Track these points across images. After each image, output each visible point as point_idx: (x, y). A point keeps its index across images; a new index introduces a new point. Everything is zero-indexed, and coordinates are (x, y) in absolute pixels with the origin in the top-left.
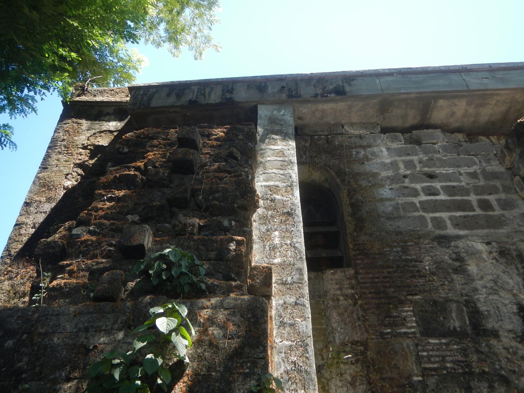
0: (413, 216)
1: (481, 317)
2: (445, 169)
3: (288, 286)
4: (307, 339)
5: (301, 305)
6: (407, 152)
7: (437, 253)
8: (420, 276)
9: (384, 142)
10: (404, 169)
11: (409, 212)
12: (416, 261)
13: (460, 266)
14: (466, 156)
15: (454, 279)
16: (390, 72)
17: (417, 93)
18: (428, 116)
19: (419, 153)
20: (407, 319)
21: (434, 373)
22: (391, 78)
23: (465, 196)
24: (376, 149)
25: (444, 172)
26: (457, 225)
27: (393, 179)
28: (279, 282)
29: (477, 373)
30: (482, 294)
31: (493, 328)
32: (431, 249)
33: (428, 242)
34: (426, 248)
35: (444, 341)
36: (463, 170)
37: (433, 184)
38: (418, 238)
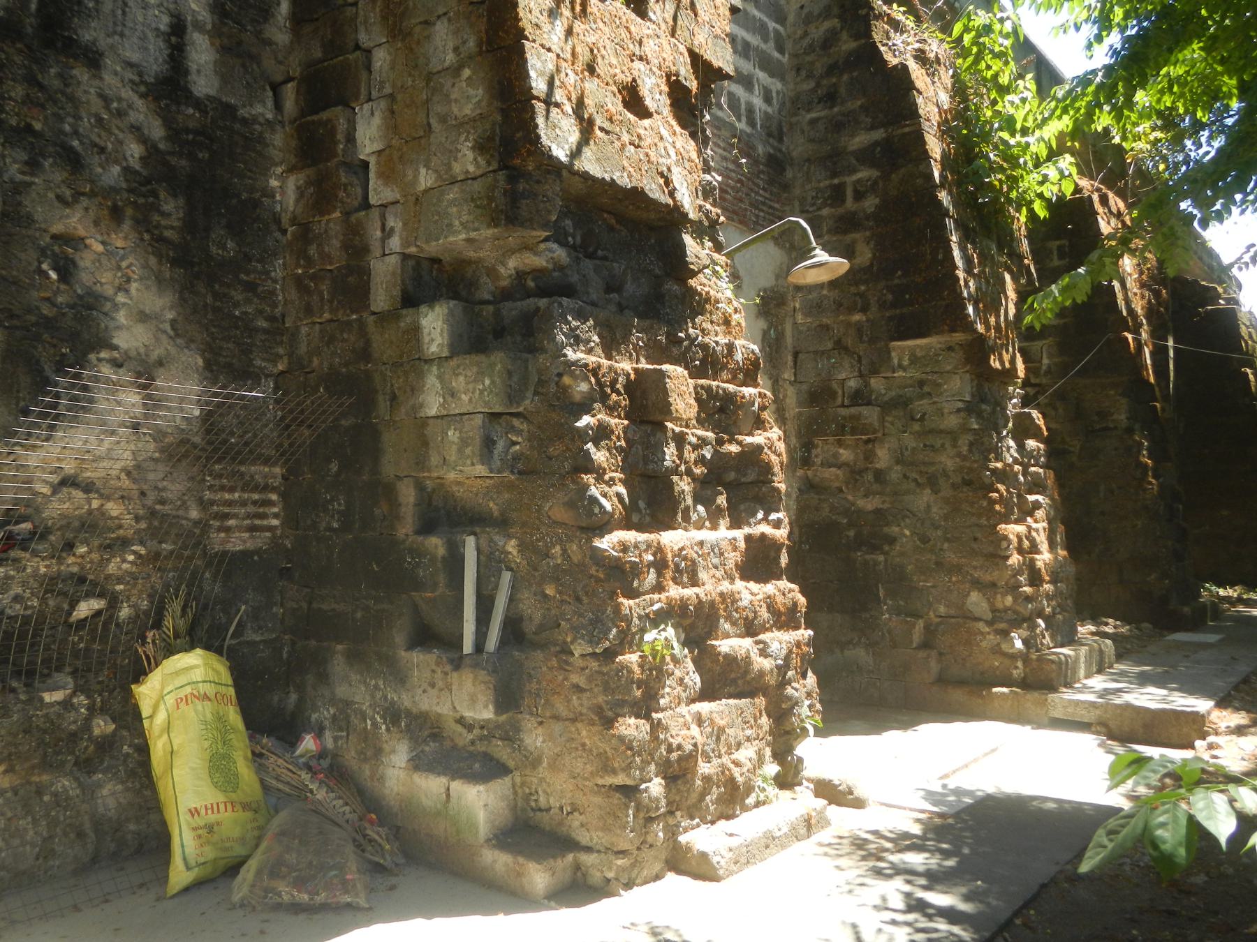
1: (76, 8)
29: (11, 126)
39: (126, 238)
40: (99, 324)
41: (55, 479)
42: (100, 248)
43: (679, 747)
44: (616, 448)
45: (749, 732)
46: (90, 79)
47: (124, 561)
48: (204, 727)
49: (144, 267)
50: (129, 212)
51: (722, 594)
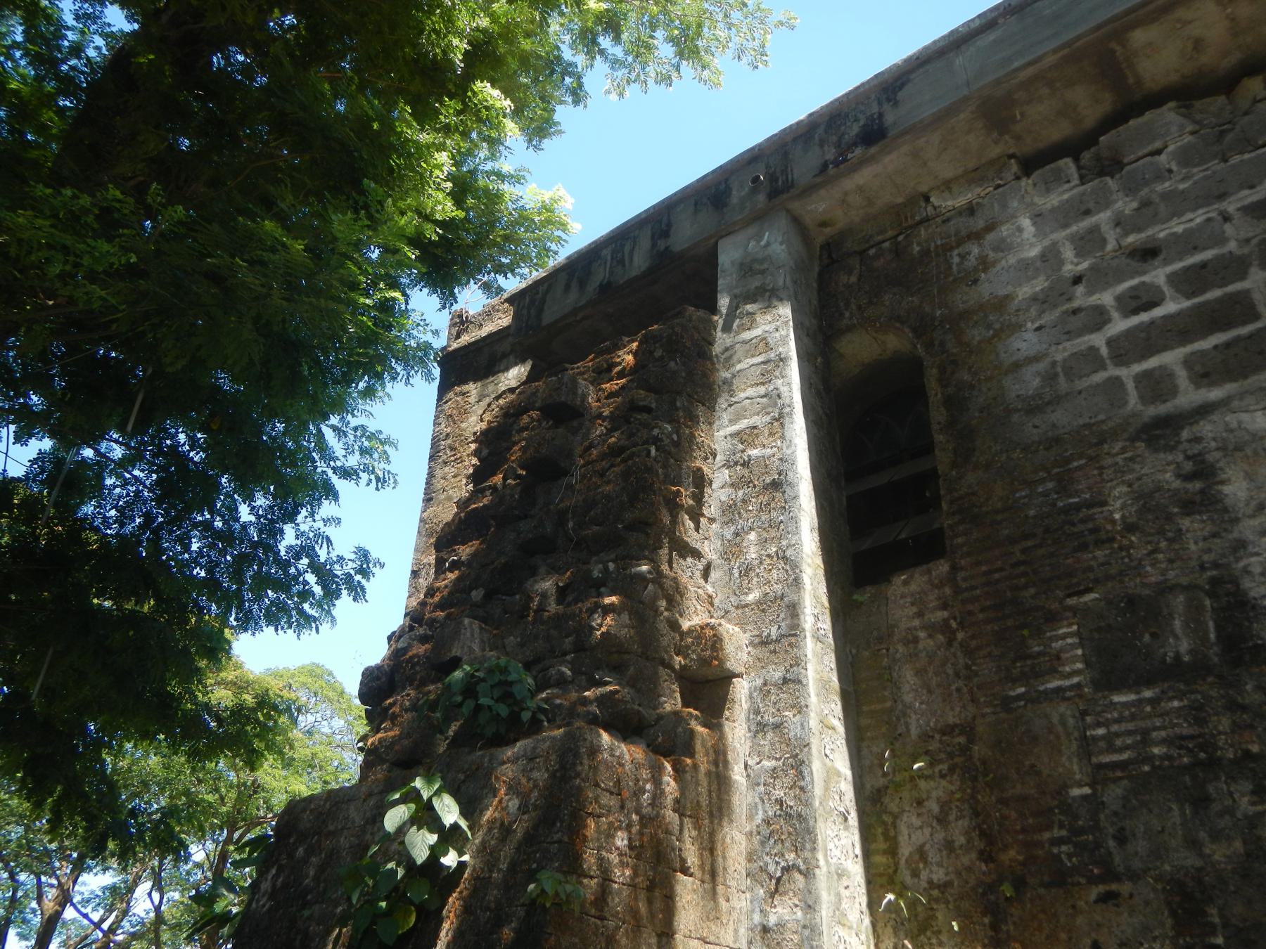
0: (1090, 386)
1: (1251, 614)
2: (1184, 219)
3: (772, 647)
4: (801, 751)
5: (794, 681)
6: (1083, 208)
7: (1143, 472)
8: (1099, 543)
9: (1028, 200)
10: (1075, 260)
11: (1081, 377)
12: (1090, 505)
13: (1202, 492)
14: (1247, 156)
15: (1184, 528)
16: (983, 21)
17: (1055, 51)
18: (1131, 81)
19: (1114, 197)
20: (1064, 656)
21: (1119, 774)
22: (991, 37)
23: (1232, 282)
24: (1008, 230)
25: (1179, 229)
26: (1204, 373)
27: (1043, 301)
28: (757, 641)
29: (1230, 760)
30: (1257, 554)
32: (1130, 464)
33: (1122, 448)
34: (1117, 463)
35: (1148, 694)
36: (1231, 206)
37: (1146, 278)
38: (1097, 444)
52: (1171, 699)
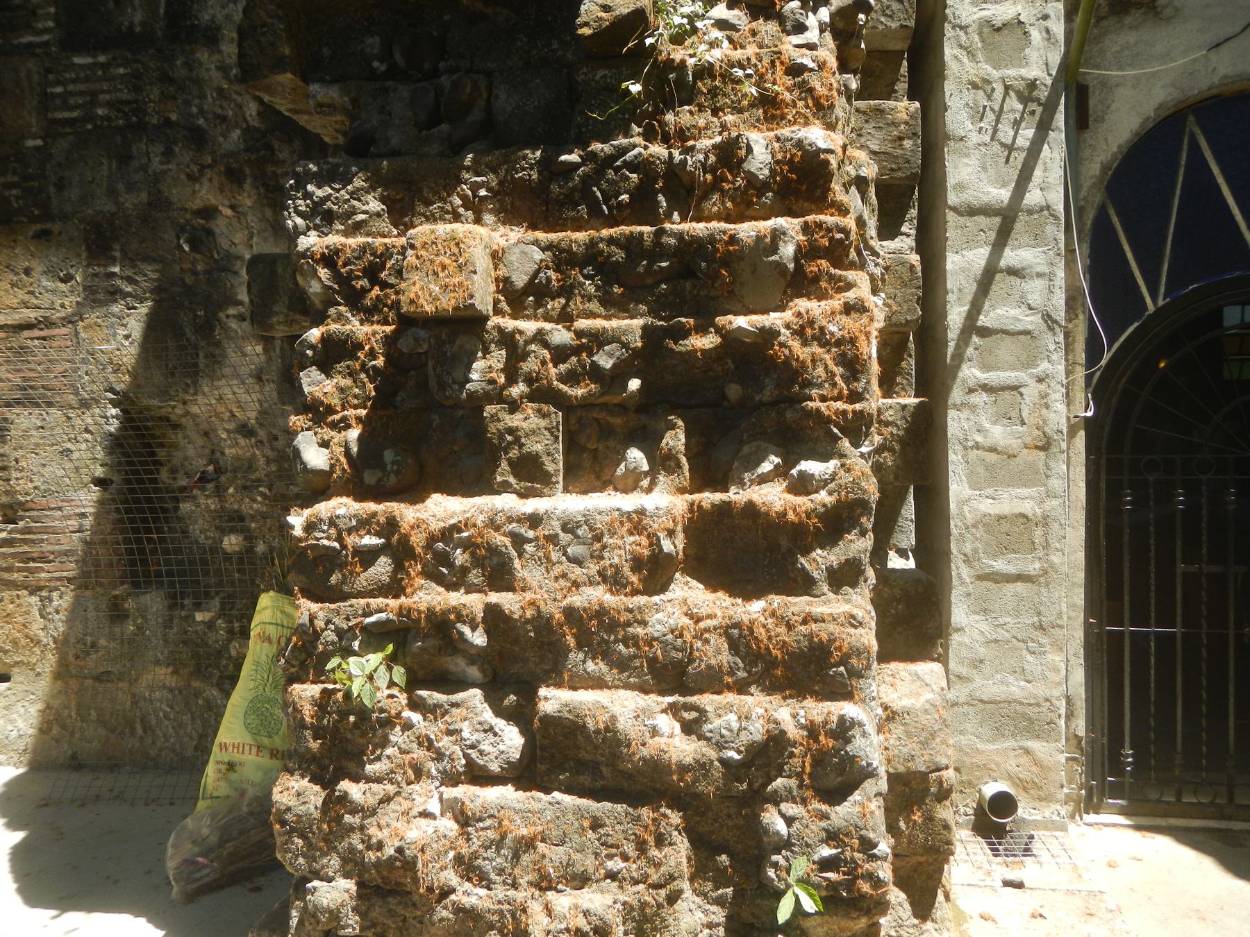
20: (40, 12)
21: (68, 130)
31: (213, 21)
35: (102, 59)
39: (249, 196)
40: (226, 284)
41: (231, 426)
42: (229, 212)
43: (380, 846)
44: (367, 372)
45: (616, 864)
46: (210, 56)
47: (255, 501)
48: (254, 667)
49: (261, 221)
50: (248, 171)
51: (569, 612)
52: (118, 66)
